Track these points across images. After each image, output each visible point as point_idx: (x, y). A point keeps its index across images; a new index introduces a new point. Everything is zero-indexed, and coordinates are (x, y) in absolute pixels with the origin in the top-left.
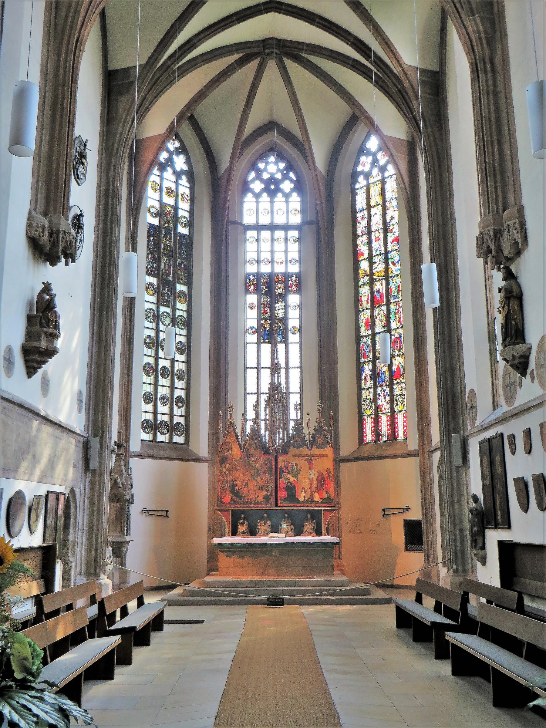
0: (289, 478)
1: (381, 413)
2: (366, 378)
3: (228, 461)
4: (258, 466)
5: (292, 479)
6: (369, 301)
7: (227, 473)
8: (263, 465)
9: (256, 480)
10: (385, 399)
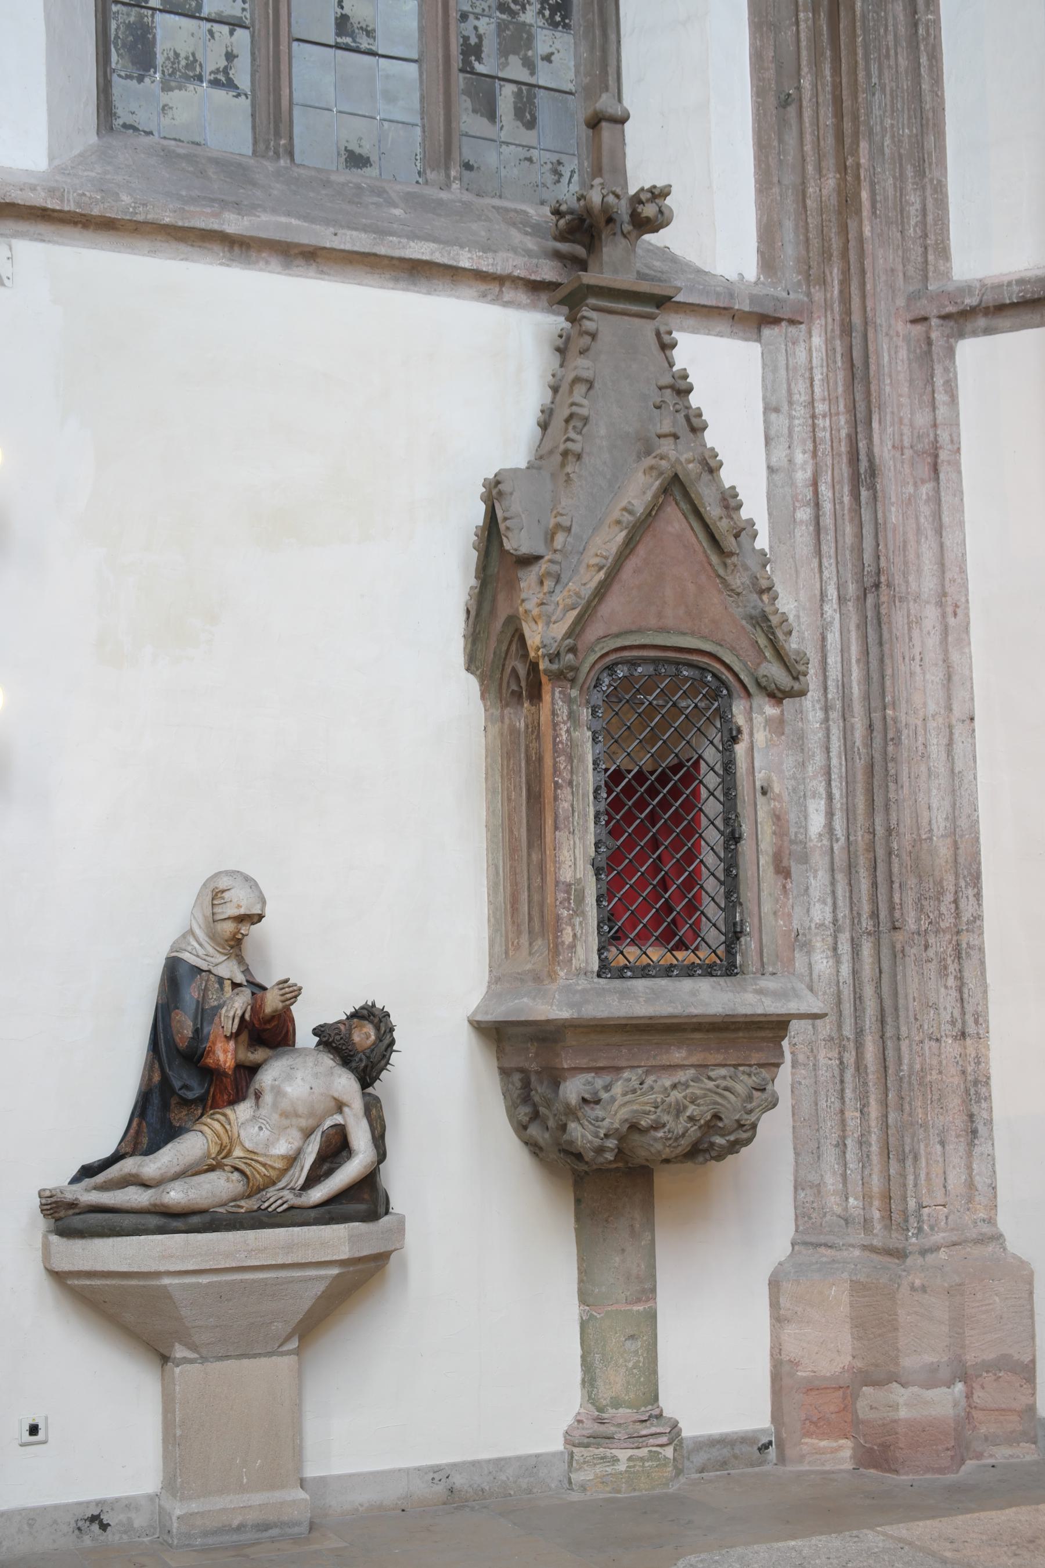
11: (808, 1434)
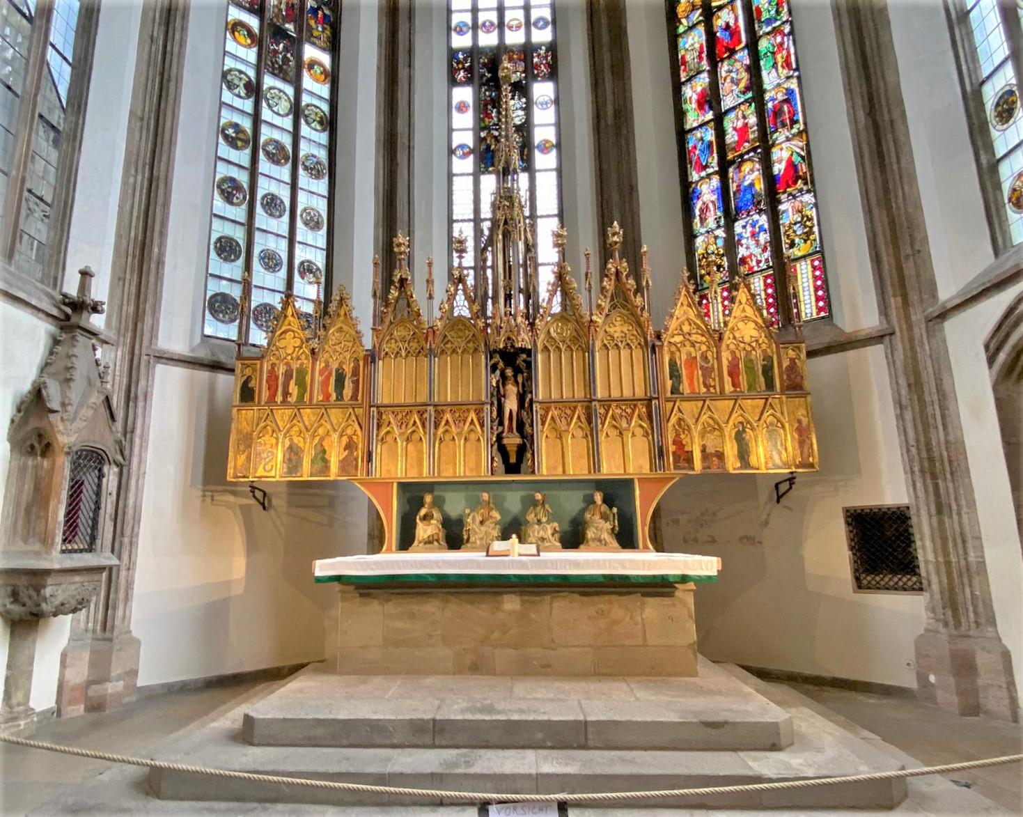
6: (704, 55)
10: (757, 242)
11: (71, 705)
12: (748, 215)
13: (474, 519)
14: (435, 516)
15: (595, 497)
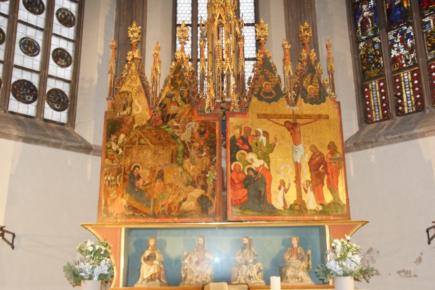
0: (252, 160)
1: (399, 71)
2: (365, 22)
3: (125, 128)
4: (185, 136)
5: (257, 163)
7: (121, 151)
8: (197, 135)
9: (181, 165)
12: (398, 27)
13: (190, 259)
14: (158, 257)
15: (293, 241)
